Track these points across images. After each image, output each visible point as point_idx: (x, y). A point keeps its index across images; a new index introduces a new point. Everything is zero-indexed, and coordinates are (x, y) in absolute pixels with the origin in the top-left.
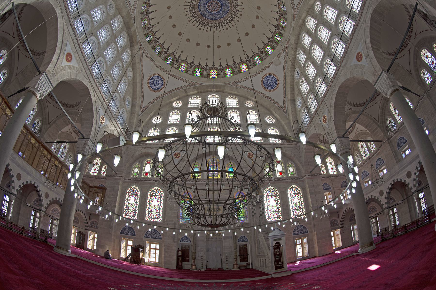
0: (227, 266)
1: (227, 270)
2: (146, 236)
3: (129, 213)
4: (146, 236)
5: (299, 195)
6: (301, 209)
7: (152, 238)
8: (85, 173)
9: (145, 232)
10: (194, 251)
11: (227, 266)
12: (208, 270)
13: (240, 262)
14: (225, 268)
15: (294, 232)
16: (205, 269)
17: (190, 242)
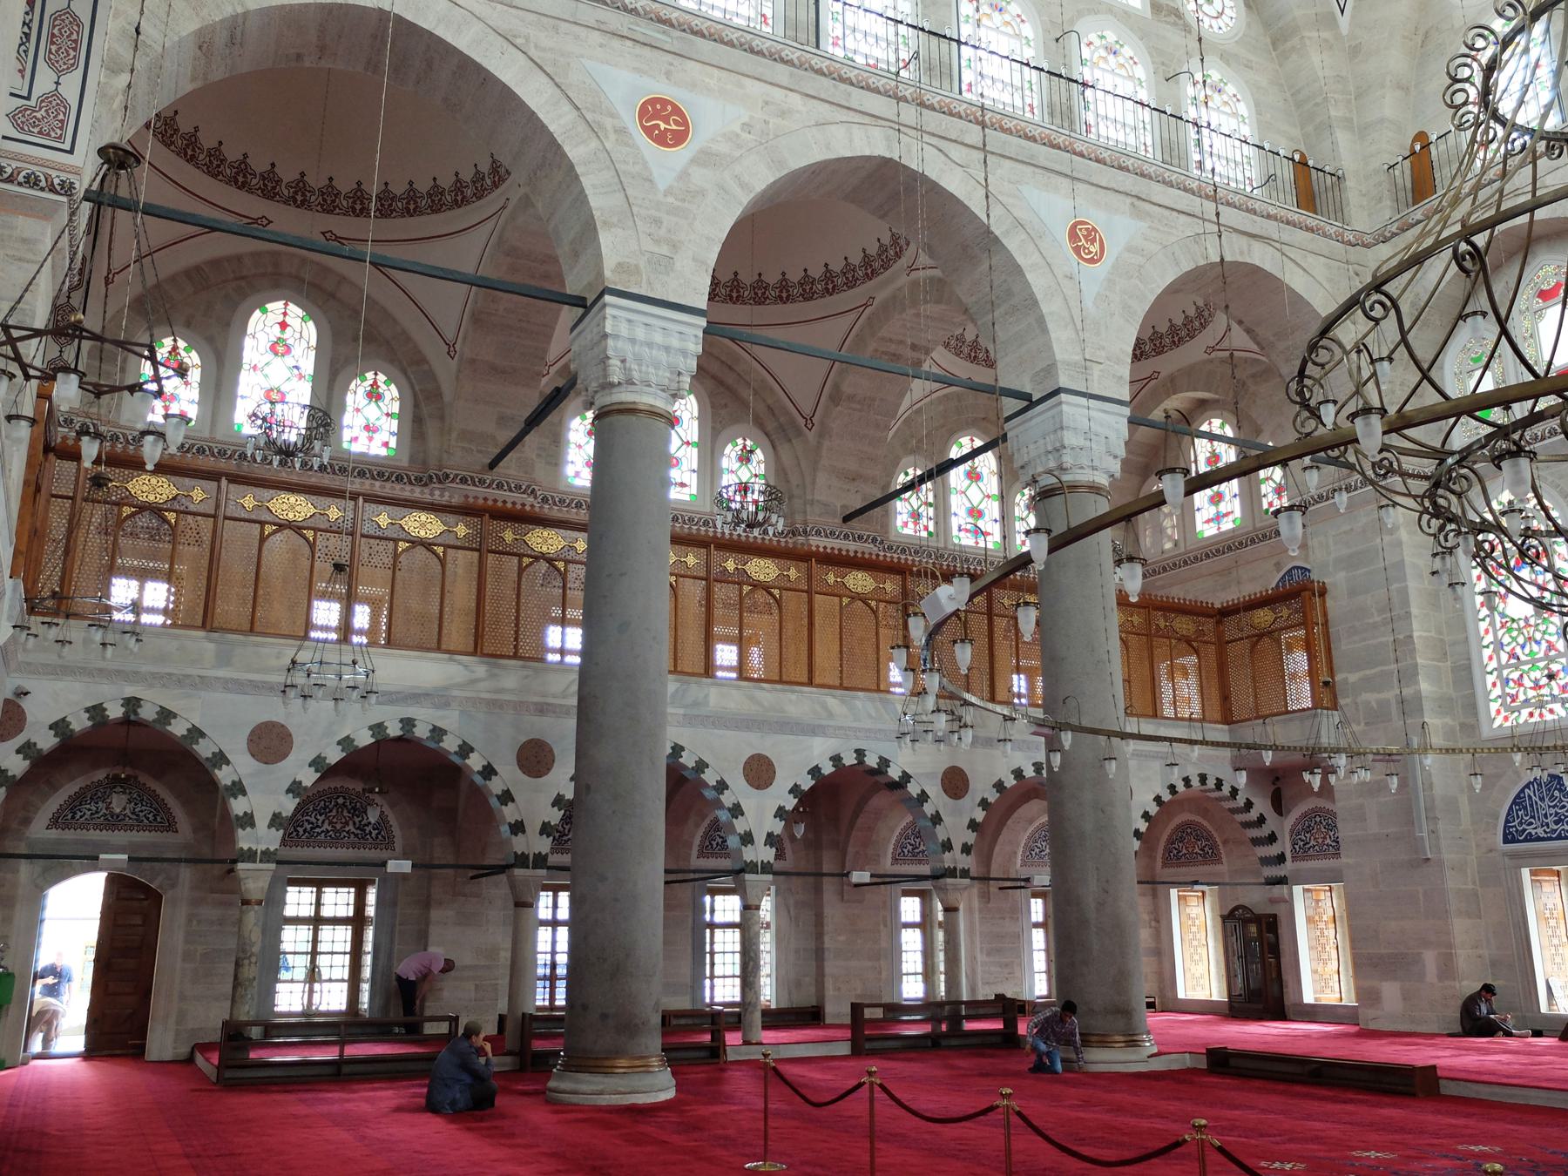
3: (1527, 683)
8: (1168, 545)
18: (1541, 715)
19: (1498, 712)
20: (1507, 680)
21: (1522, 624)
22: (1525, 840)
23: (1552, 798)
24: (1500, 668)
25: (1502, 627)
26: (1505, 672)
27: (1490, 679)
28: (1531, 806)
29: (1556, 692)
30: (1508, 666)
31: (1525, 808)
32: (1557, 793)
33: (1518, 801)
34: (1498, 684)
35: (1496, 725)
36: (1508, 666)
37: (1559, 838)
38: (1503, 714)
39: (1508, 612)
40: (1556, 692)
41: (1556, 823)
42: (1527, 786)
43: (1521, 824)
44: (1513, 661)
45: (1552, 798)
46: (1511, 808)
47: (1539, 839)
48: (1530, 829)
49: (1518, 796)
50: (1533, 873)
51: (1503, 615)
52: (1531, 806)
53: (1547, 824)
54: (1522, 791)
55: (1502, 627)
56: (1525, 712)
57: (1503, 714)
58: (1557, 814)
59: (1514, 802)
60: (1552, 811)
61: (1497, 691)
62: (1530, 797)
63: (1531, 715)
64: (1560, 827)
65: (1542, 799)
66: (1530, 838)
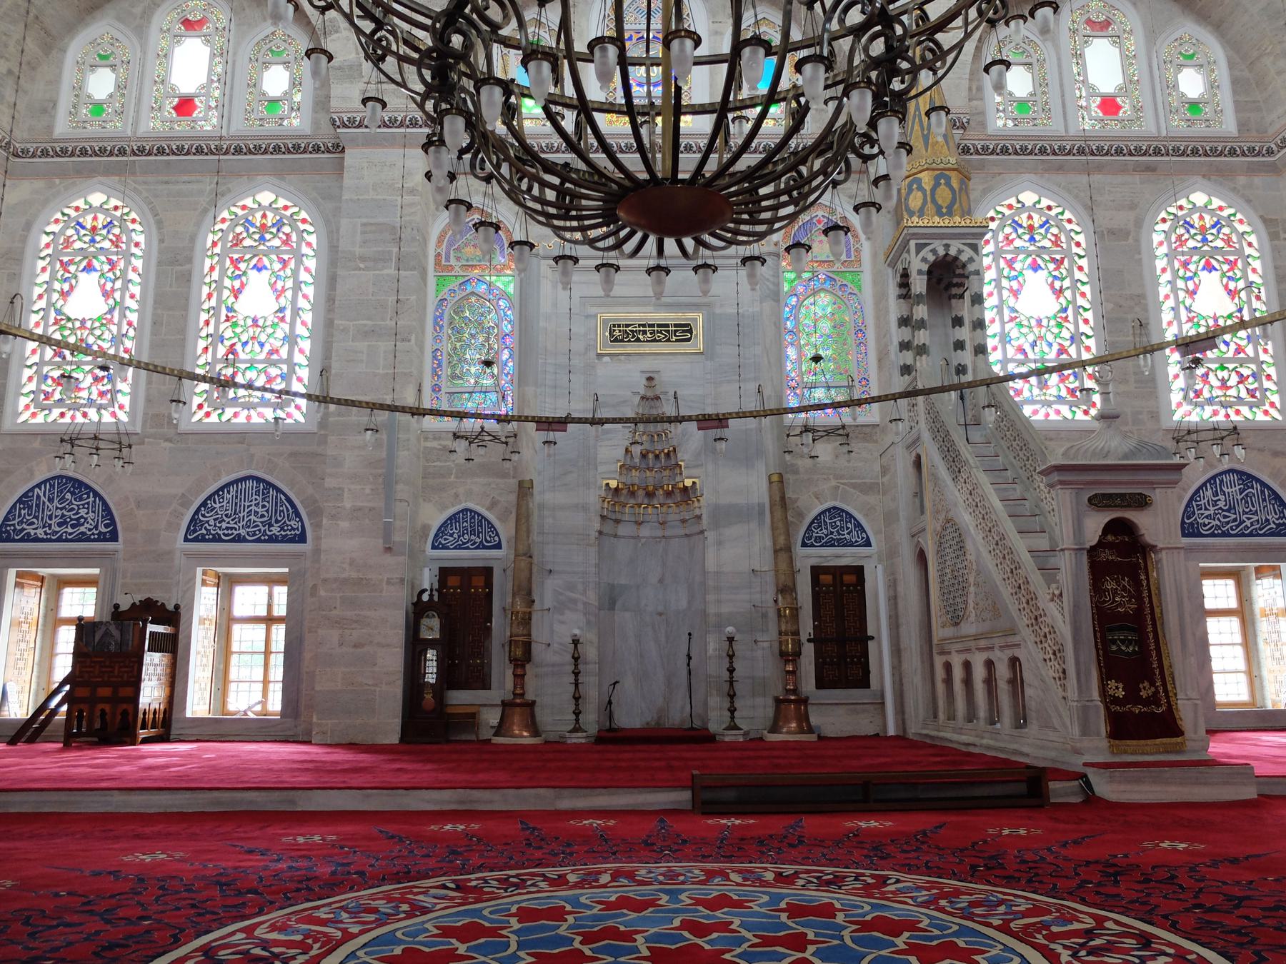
0: (732, 710)
1: (730, 737)
2: (195, 532)
4: (195, 532)
5: (1233, 265)
6: (1249, 360)
7: (239, 539)
9: (185, 504)
10: (520, 607)
11: (732, 710)
12: (611, 737)
13: (821, 684)
14: (716, 723)
15: (1188, 512)
16: (593, 730)
17: (498, 546)
18: (73, 417)
19: (27, 407)
20: (46, 377)
21: (78, 324)
22: (21, 540)
23: (62, 500)
24: (41, 363)
25: (55, 323)
26: (46, 369)
27: (27, 373)
28: (38, 506)
29: (94, 396)
30: (50, 363)
31: (30, 508)
32: (68, 496)
33: (24, 500)
34: (35, 379)
35: (20, 420)
36: (50, 363)
37: (59, 540)
38: (32, 410)
39: (66, 310)
40: (94, 396)
41: (60, 525)
42: (39, 486)
43: (21, 523)
44: (58, 359)
45: (62, 500)
46: (15, 504)
47: (37, 540)
48: (30, 530)
49: (25, 495)
50: (19, 575)
51: (58, 312)
52: (38, 506)
53: (50, 526)
54: (32, 490)
55: (55, 323)
56: (56, 412)
57: (32, 410)
58: (63, 515)
59: (19, 501)
60: (59, 513)
61: (32, 386)
62: (38, 497)
63: (62, 415)
64: (63, 530)
65: (51, 500)
66: (28, 538)
